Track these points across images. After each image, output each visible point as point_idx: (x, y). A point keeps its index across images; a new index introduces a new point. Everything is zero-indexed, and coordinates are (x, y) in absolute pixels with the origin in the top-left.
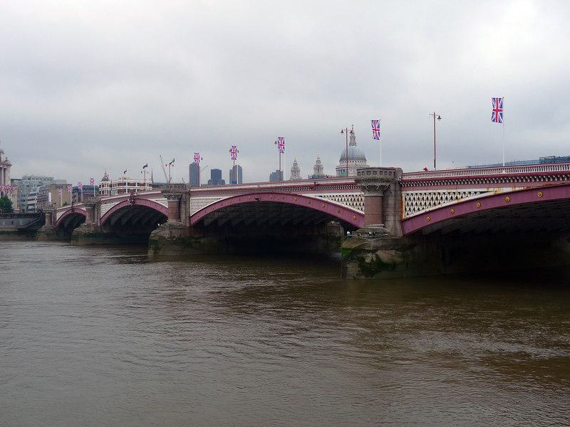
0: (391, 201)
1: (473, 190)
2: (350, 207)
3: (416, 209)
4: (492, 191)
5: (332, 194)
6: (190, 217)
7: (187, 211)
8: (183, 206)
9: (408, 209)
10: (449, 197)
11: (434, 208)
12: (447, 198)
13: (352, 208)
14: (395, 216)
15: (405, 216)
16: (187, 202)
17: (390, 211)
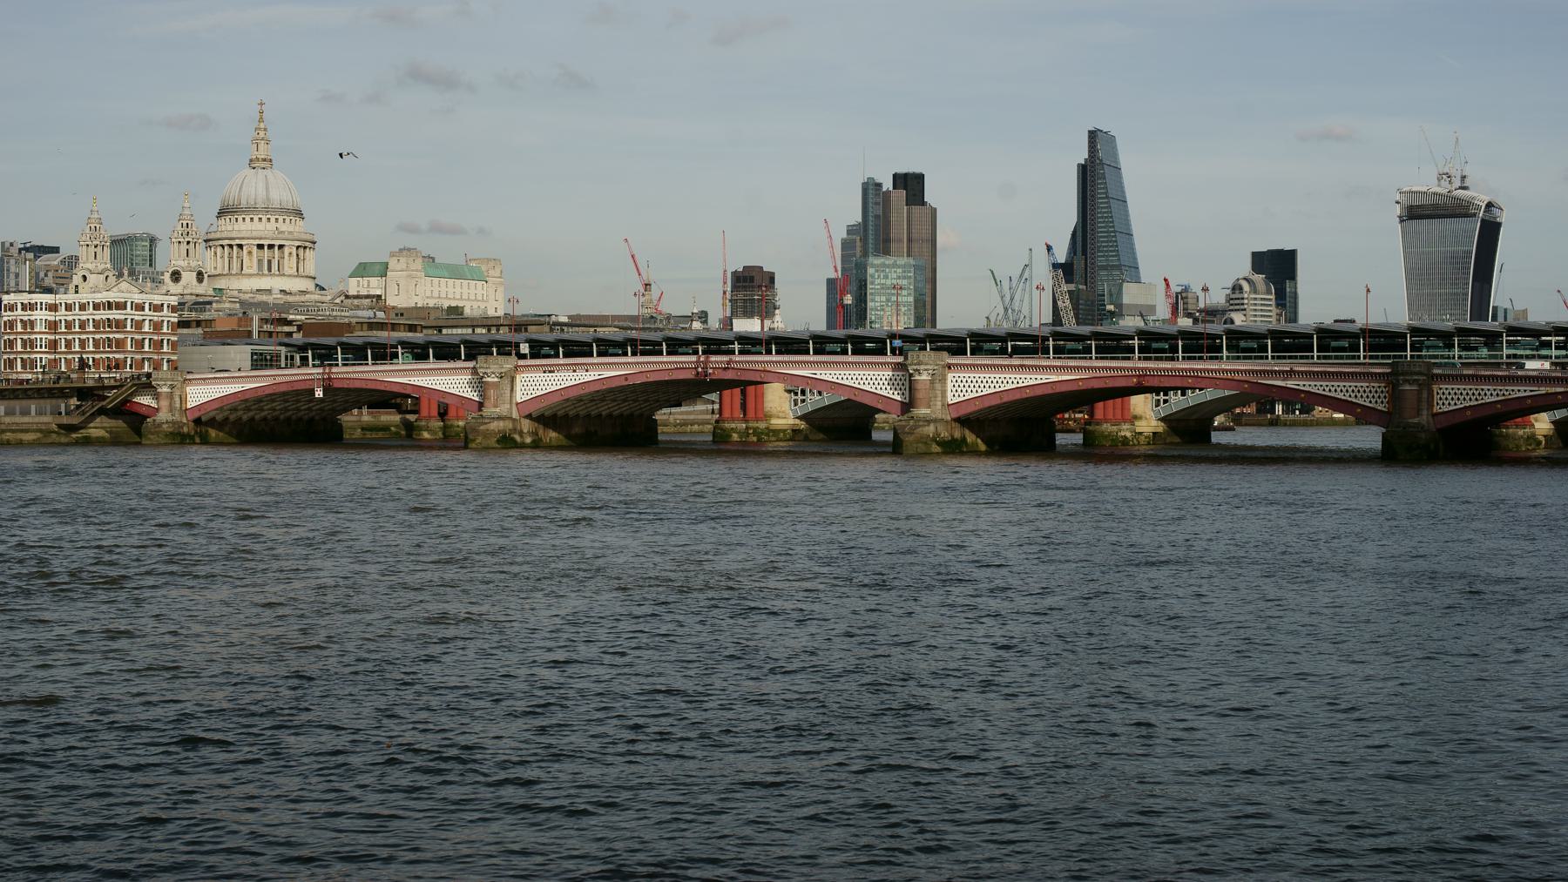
0: (1425, 395)
1: (1522, 388)
2: (1350, 399)
3: (1452, 403)
4: (1543, 390)
5: (1318, 383)
6: (949, 405)
7: (944, 393)
8: (938, 386)
9: (1440, 403)
10: (1495, 393)
11: (1476, 403)
12: (1491, 395)
13: (1354, 400)
14: (1428, 409)
15: (1436, 409)
16: (943, 380)
17: (1424, 405)
